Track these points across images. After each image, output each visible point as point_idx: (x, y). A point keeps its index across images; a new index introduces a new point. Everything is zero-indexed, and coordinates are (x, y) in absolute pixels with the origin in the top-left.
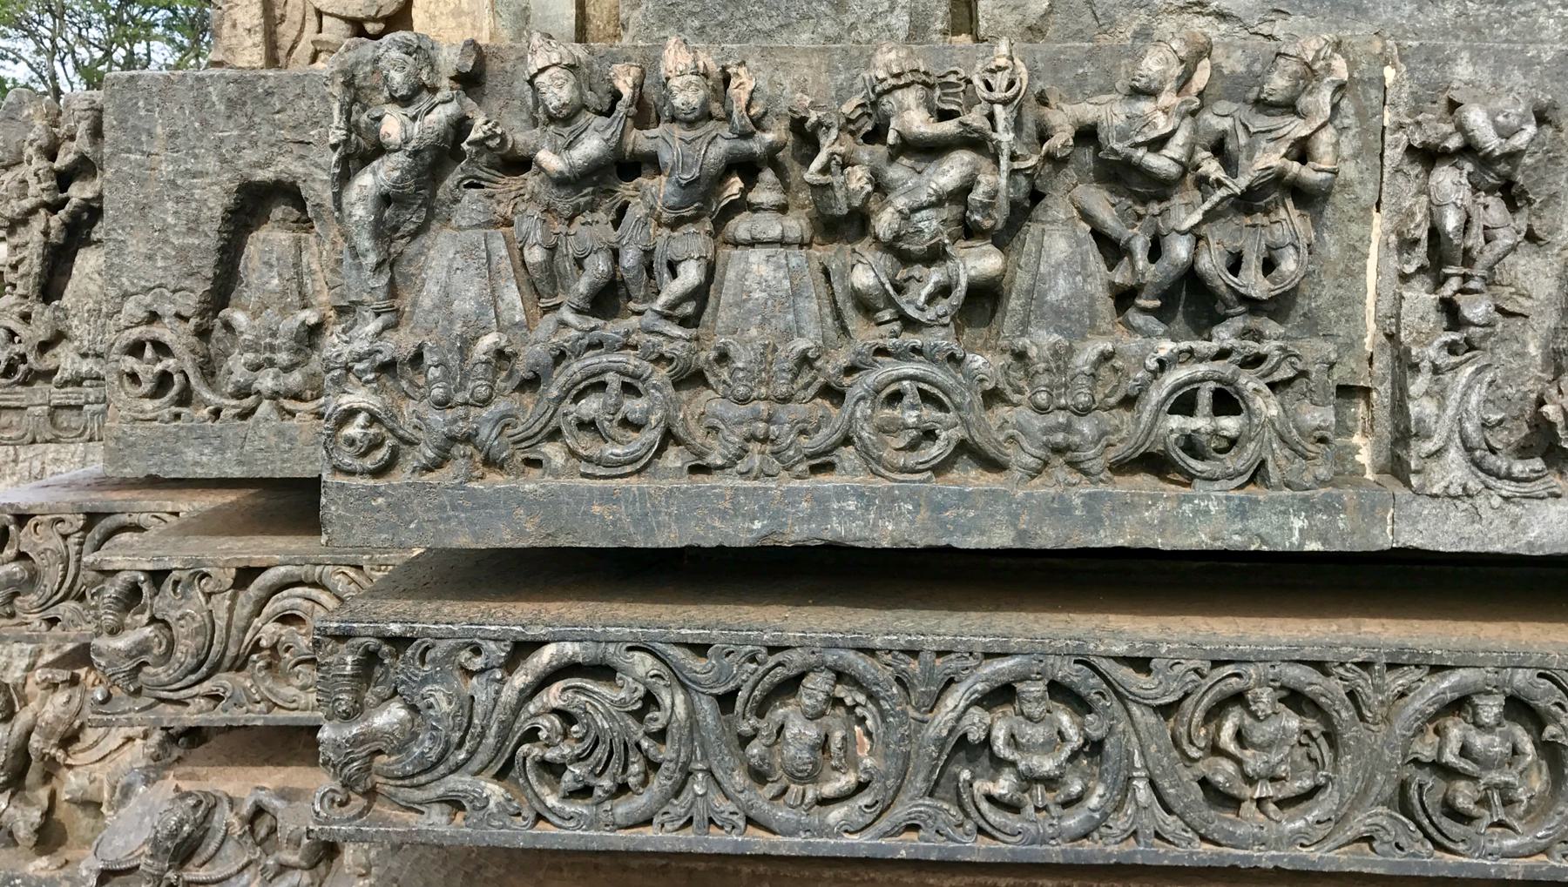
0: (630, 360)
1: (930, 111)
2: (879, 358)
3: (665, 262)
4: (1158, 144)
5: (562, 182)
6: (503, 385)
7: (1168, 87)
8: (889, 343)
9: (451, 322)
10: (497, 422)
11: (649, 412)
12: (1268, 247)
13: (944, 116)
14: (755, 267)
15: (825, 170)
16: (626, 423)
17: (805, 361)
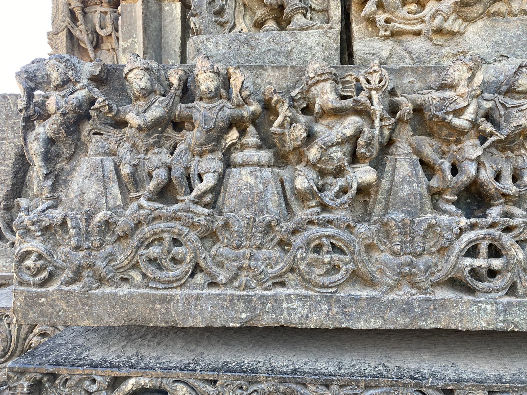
0: (176, 225)
1: (337, 95)
2: (310, 227)
3: (196, 173)
4: (459, 113)
5: (140, 129)
6: (110, 239)
7: (463, 83)
8: (315, 217)
9: (82, 205)
10: (106, 258)
11: (185, 255)
12: (514, 168)
13: (344, 98)
14: (244, 177)
15: (281, 126)
16: (174, 260)
17: (269, 227)
